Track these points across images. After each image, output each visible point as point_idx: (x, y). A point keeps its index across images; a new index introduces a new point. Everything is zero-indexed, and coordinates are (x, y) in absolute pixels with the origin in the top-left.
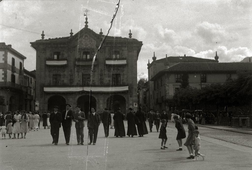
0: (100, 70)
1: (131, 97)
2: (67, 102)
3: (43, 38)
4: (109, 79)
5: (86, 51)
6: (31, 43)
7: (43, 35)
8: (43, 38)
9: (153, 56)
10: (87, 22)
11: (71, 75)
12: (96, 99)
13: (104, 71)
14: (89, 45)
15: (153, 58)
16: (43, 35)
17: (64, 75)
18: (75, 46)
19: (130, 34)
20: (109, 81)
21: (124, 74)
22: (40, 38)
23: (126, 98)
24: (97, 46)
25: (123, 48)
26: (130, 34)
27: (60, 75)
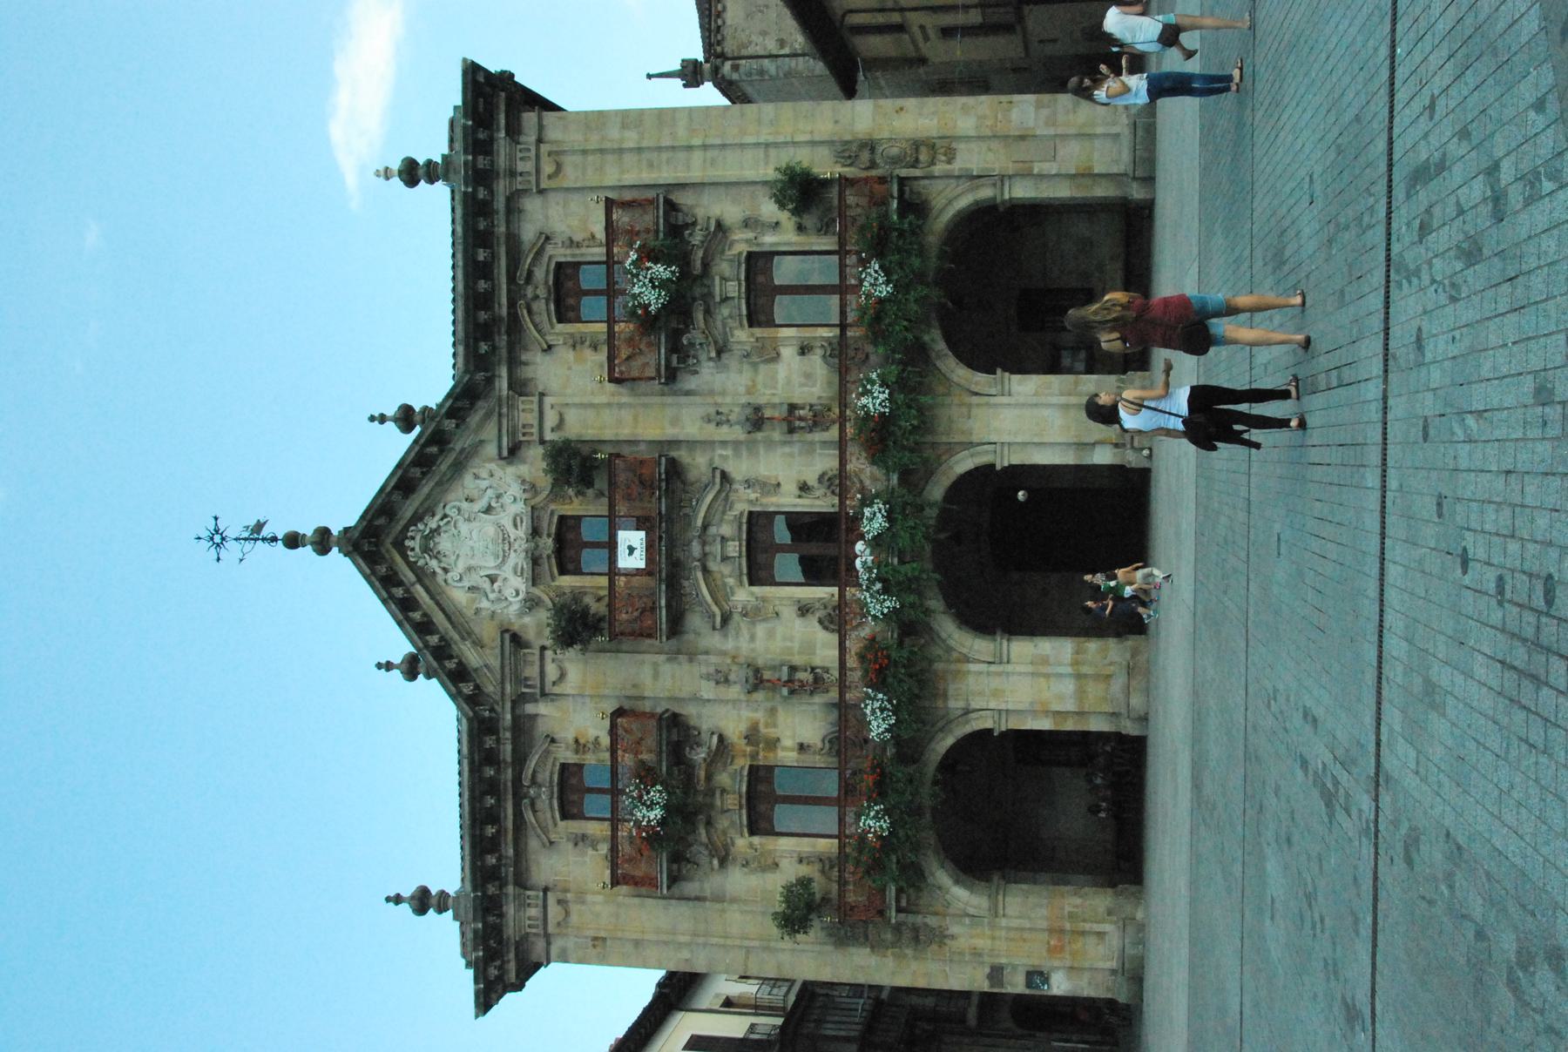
0: (712, 426)
1: (951, 156)
2: (988, 724)
3: (442, 903)
4: (788, 352)
5: (547, 544)
6: (485, 1002)
7: (423, 901)
8: (442, 903)
9: (679, 82)
10: (323, 541)
11: (757, 680)
12: (963, 464)
13: (719, 400)
14: (507, 523)
15: (685, 86)
16: (423, 901)
17: (752, 736)
18: (507, 636)
19: (412, 173)
20: (804, 350)
21: (746, 224)
22: (445, 930)
23: (964, 202)
24: (505, 453)
25: (528, 233)
26: (412, 173)
27: (754, 770)
